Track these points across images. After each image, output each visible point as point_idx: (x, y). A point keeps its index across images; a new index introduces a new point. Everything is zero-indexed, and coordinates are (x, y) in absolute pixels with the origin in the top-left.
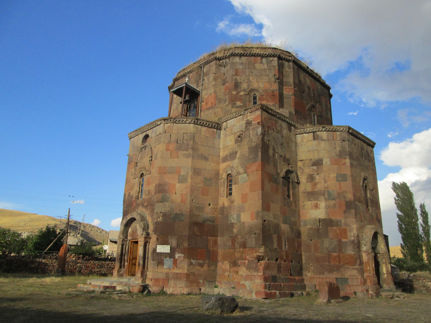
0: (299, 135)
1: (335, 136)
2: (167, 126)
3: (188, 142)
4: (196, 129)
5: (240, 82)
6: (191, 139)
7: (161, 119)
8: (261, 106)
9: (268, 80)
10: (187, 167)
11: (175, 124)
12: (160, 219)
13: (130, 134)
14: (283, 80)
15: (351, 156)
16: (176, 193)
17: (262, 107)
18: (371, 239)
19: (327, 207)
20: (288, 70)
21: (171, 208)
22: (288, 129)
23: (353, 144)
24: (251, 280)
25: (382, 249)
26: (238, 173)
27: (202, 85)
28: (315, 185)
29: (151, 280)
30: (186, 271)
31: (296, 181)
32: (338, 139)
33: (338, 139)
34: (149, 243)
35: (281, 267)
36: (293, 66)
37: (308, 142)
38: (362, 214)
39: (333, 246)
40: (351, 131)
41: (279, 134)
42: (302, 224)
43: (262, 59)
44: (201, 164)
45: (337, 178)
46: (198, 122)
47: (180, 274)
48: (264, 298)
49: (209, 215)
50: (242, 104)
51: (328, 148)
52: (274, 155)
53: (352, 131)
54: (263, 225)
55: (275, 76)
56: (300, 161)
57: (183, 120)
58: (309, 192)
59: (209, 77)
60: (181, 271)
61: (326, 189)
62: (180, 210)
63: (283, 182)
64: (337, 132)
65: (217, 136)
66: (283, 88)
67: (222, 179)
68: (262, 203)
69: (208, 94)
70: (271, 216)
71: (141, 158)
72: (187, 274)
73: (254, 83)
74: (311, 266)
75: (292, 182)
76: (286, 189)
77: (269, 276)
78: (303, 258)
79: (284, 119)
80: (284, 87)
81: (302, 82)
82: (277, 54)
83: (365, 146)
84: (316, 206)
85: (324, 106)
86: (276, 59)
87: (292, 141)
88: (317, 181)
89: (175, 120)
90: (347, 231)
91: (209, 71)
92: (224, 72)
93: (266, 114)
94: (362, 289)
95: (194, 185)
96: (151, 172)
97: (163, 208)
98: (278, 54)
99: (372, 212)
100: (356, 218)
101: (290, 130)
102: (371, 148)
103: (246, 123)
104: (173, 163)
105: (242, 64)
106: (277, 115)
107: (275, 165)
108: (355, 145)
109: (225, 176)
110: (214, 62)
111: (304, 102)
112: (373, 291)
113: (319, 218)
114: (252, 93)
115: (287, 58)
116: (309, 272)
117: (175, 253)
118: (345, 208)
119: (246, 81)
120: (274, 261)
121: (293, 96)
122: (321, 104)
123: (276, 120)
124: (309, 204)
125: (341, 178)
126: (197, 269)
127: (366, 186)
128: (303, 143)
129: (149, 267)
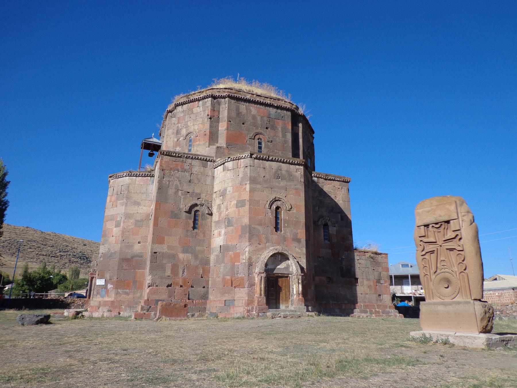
0: (216, 169)
1: (239, 164)
14: (218, 117)
15: (253, 181)
16: (113, 236)
17: (162, 153)
18: (266, 261)
19: (226, 234)
30: (113, 299)
31: (207, 212)
34: (95, 278)
40: (255, 156)
41: (186, 172)
42: (211, 251)
44: (133, 209)
51: (232, 177)
52: (176, 193)
55: (208, 115)
63: (186, 216)
65: (150, 183)
72: (112, 301)
74: (213, 290)
75: (203, 214)
76: (191, 222)
77: (151, 300)
79: (195, 157)
82: (210, 95)
84: (220, 235)
85: (280, 129)
86: (210, 99)
93: (169, 157)
95: (125, 227)
98: (211, 94)
99: (285, 233)
100: (249, 242)
101: (205, 166)
106: (184, 156)
115: (222, 95)
119: (185, 127)
121: (226, 131)
125: (240, 204)
127: (278, 208)
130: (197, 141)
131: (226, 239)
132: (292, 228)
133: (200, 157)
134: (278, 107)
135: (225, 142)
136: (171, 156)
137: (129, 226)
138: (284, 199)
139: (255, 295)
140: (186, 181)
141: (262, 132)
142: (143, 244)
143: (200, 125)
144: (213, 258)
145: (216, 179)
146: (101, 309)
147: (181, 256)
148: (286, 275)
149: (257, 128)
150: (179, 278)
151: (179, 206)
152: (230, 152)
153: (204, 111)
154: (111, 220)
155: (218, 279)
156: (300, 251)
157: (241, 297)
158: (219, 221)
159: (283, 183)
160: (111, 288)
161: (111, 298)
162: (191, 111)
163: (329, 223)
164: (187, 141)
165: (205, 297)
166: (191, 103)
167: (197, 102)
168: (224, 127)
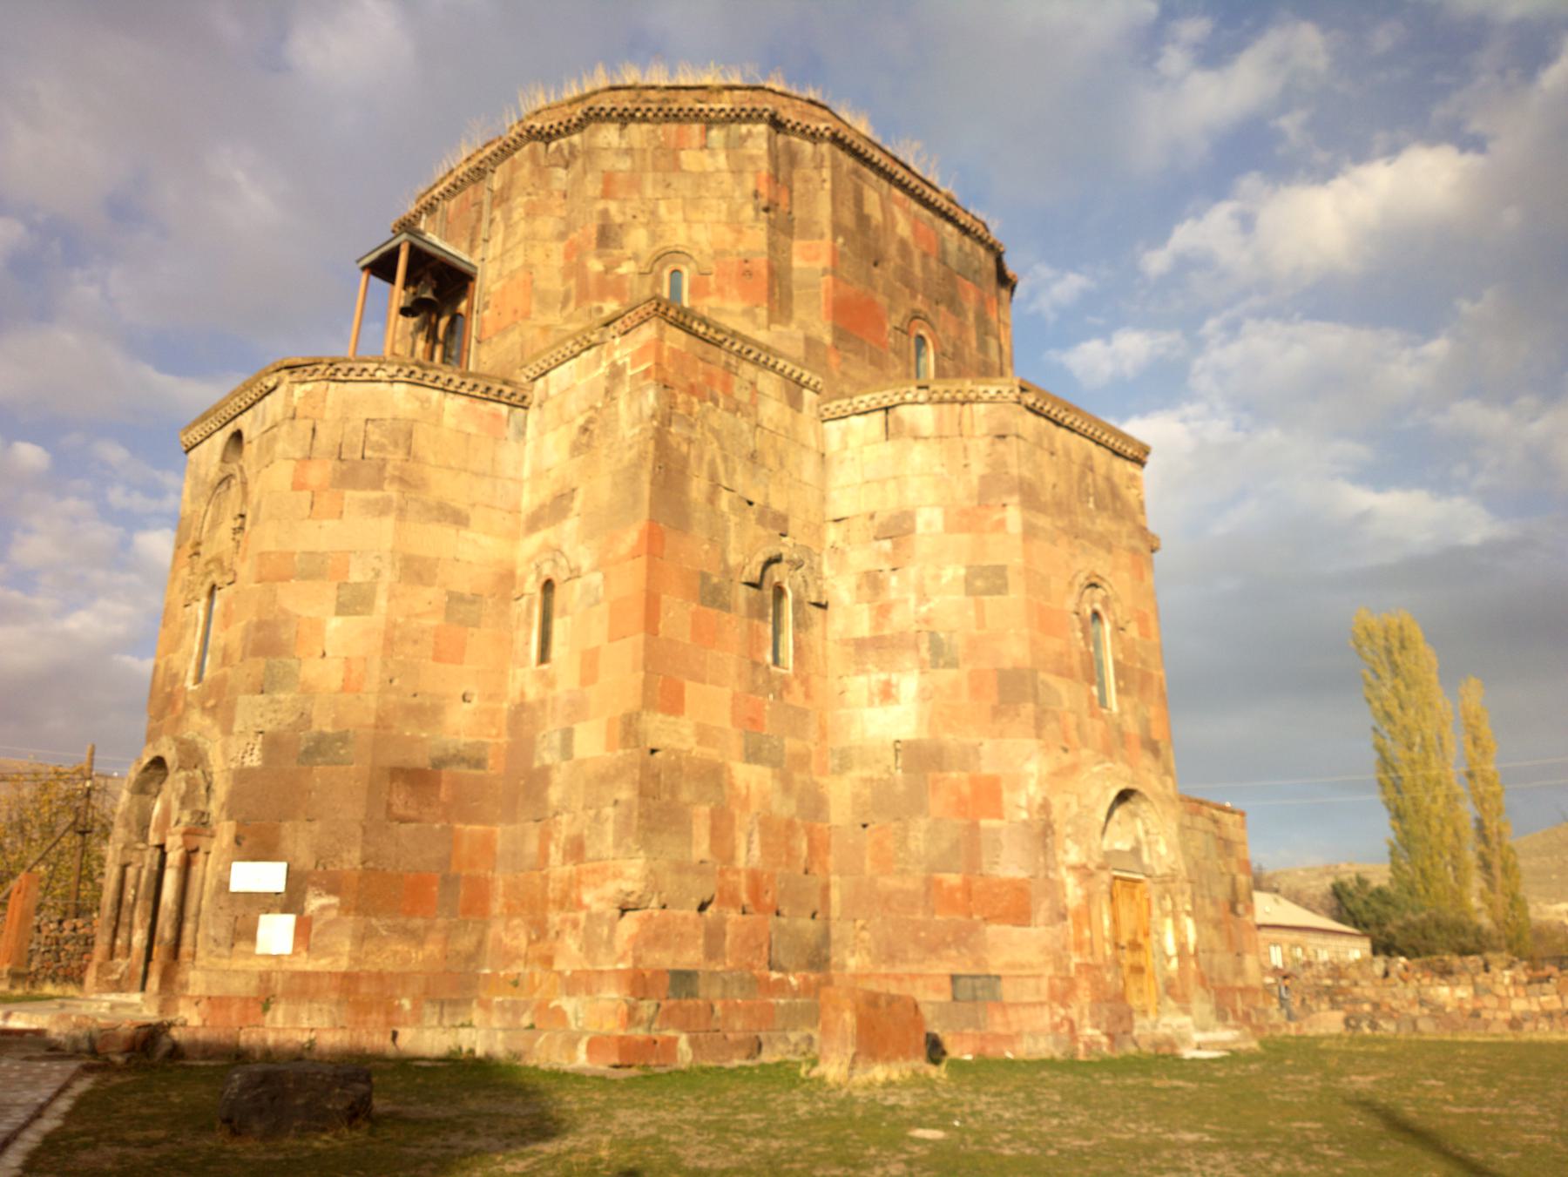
1: (966, 421)
2: (302, 395)
3: (382, 455)
4: (417, 404)
5: (621, 226)
6: (396, 444)
7: (278, 366)
8: (659, 305)
10: (376, 554)
11: (333, 385)
12: (254, 760)
14: (790, 213)
15: (1029, 495)
17: (662, 309)
19: (924, 695)
20: (813, 174)
21: (302, 714)
22: (785, 398)
23: (1039, 452)
24: (589, 992)
25: (1160, 857)
26: (575, 574)
27: (486, 241)
28: (883, 611)
29: (197, 1004)
30: (343, 965)
31: (814, 600)
32: (978, 432)
33: (981, 429)
34: (207, 853)
35: (724, 934)
36: (834, 158)
37: (866, 449)
38: (1071, 720)
41: (743, 416)
43: (708, 129)
44: (433, 539)
45: (968, 582)
46: (424, 375)
47: (316, 975)
48: (616, 1067)
49: (464, 739)
51: (938, 469)
52: (712, 499)
53: (1038, 400)
54: (644, 767)
55: (756, 195)
56: (837, 521)
57: (364, 370)
59: (510, 211)
60: (323, 964)
61: (924, 627)
62: (336, 722)
63: (750, 602)
64: (975, 406)
65: (510, 432)
66: (790, 248)
67: (523, 595)
68: (647, 685)
69: (505, 272)
71: (215, 524)
72: (346, 976)
74: (863, 928)
77: (657, 973)
78: (835, 896)
80: (797, 245)
81: (874, 223)
83: (1100, 455)
84: (887, 693)
85: (971, 316)
86: (762, 128)
87: (803, 446)
88: (893, 595)
89: (332, 370)
90: (1004, 787)
91: (508, 186)
92: (564, 188)
94: (1052, 1017)
95: (400, 620)
96: (235, 574)
97: (273, 716)
98: (770, 107)
99: (1121, 714)
101: (795, 402)
102: (1130, 468)
103: (607, 377)
104: (321, 535)
105: (629, 151)
107: (717, 537)
108: (1052, 454)
109: (532, 587)
110: (526, 148)
111: (882, 300)
112: (1097, 1026)
113: (896, 737)
114: (662, 268)
115: (808, 127)
116: (853, 953)
117: (304, 892)
120: (692, 913)
121: (829, 278)
122: (954, 304)
123: (728, 364)
124: (860, 685)
126: (393, 955)
128: (848, 454)
129: (201, 953)
130: (708, 294)
132: (1136, 699)
135: (829, 322)
137: (418, 616)
139: (1070, 958)
140: (744, 452)
143: (722, 229)
144: (841, 793)
149: (913, 297)
150: (737, 872)
151: (724, 552)
153: (737, 172)
155: (890, 883)
156: (1160, 788)
159: (1102, 524)
160: (323, 908)
161: (338, 956)
162: (668, 160)
165: (818, 958)
167: (696, 128)
168: (817, 258)
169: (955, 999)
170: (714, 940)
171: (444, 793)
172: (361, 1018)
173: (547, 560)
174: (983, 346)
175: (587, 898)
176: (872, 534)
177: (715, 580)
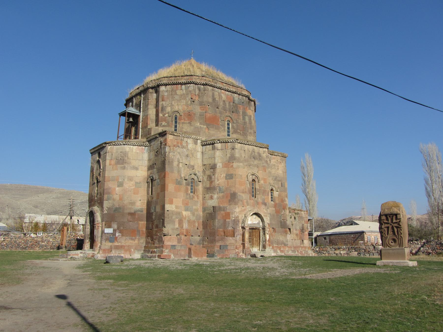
3: (123, 158)
9: (186, 103)
11: (115, 146)
13: (90, 150)
19: (218, 198)
28: (211, 182)
32: (229, 148)
38: (245, 201)
39: (220, 224)
45: (226, 177)
49: (139, 207)
50: (166, 124)
51: (221, 156)
52: (178, 165)
58: (208, 188)
61: (218, 186)
62: (119, 205)
63: (186, 183)
70: (174, 207)
73: (175, 106)
81: (217, 99)
84: (212, 198)
85: (241, 113)
95: (128, 188)
97: (108, 204)
101: (196, 143)
111: (219, 115)
118: (229, 198)
119: (169, 105)
120: (175, 236)
130: (182, 120)
131: (218, 202)
132: (261, 195)
133: (193, 136)
134: (239, 94)
136: (174, 135)
137: (131, 187)
138: (257, 174)
141: (230, 115)
142: (143, 201)
143: (184, 106)
145: (204, 154)
146: (113, 252)
147: (184, 213)
148: (258, 228)
150: (184, 230)
151: (181, 174)
152: (209, 132)
154: (113, 180)
156: (266, 211)
157: (232, 244)
158: (209, 188)
159: (256, 162)
160: (120, 235)
163: (274, 189)
164: (172, 118)
166: (174, 85)
167: (179, 85)
169: (220, 249)
170: (179, 241)
171: (136, 217)
172: (126, 252)
173: (152, 176)
174: (244, 119)
175: (158, 234)
176: (210, 168)
177: (179, 180)
